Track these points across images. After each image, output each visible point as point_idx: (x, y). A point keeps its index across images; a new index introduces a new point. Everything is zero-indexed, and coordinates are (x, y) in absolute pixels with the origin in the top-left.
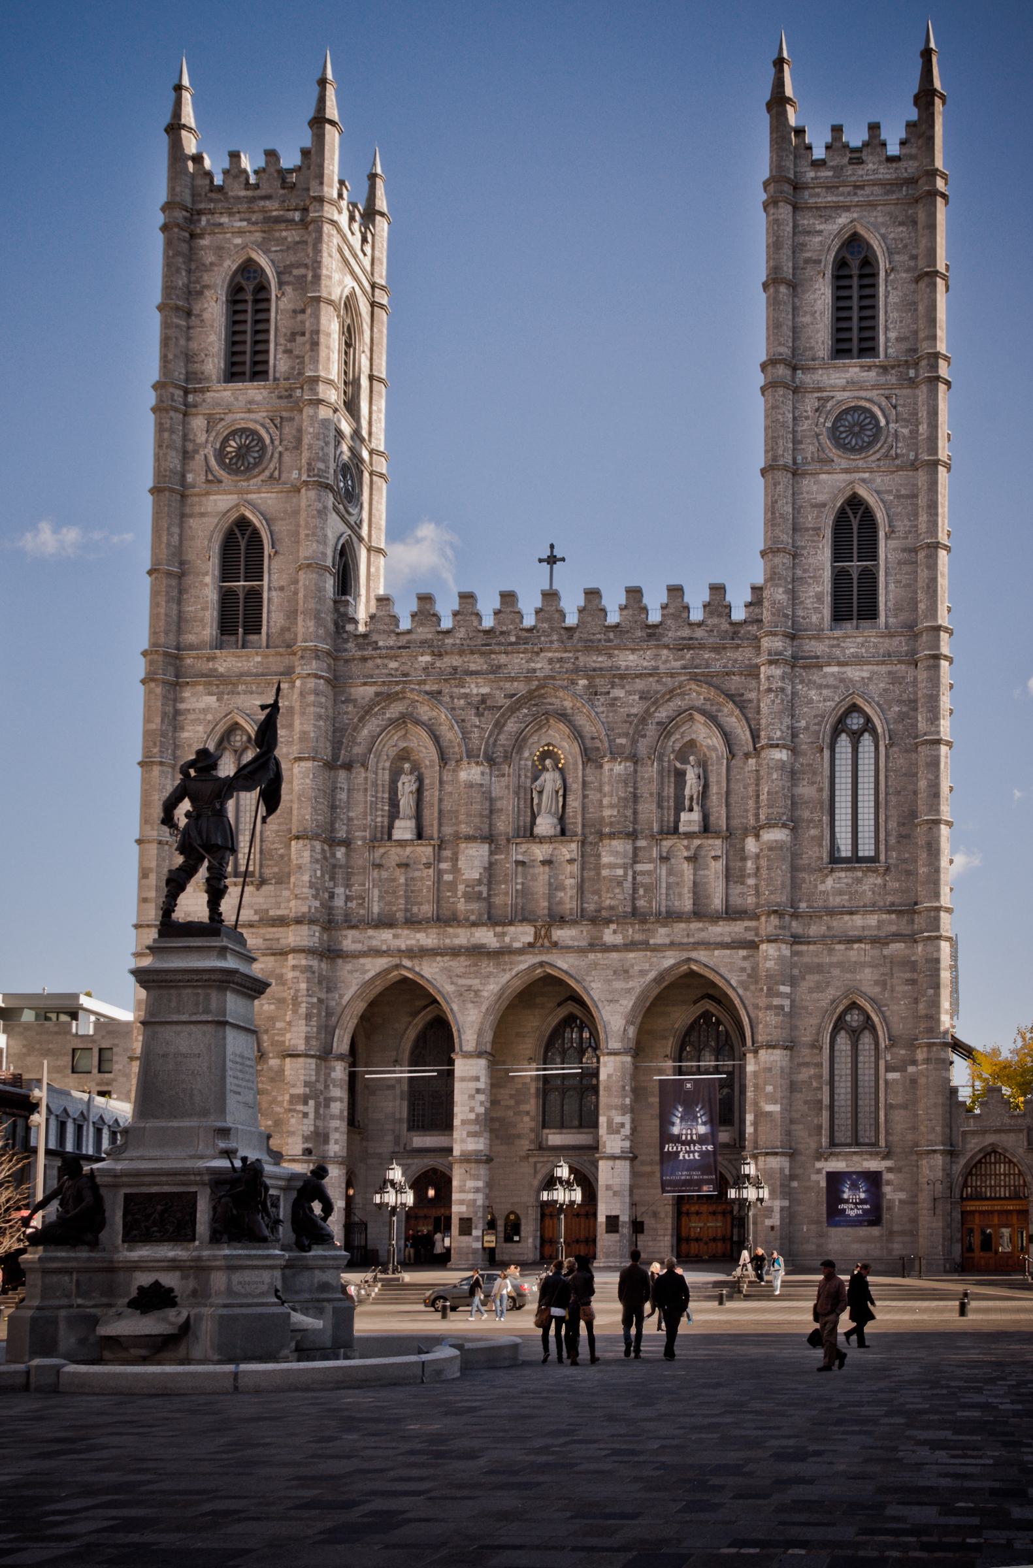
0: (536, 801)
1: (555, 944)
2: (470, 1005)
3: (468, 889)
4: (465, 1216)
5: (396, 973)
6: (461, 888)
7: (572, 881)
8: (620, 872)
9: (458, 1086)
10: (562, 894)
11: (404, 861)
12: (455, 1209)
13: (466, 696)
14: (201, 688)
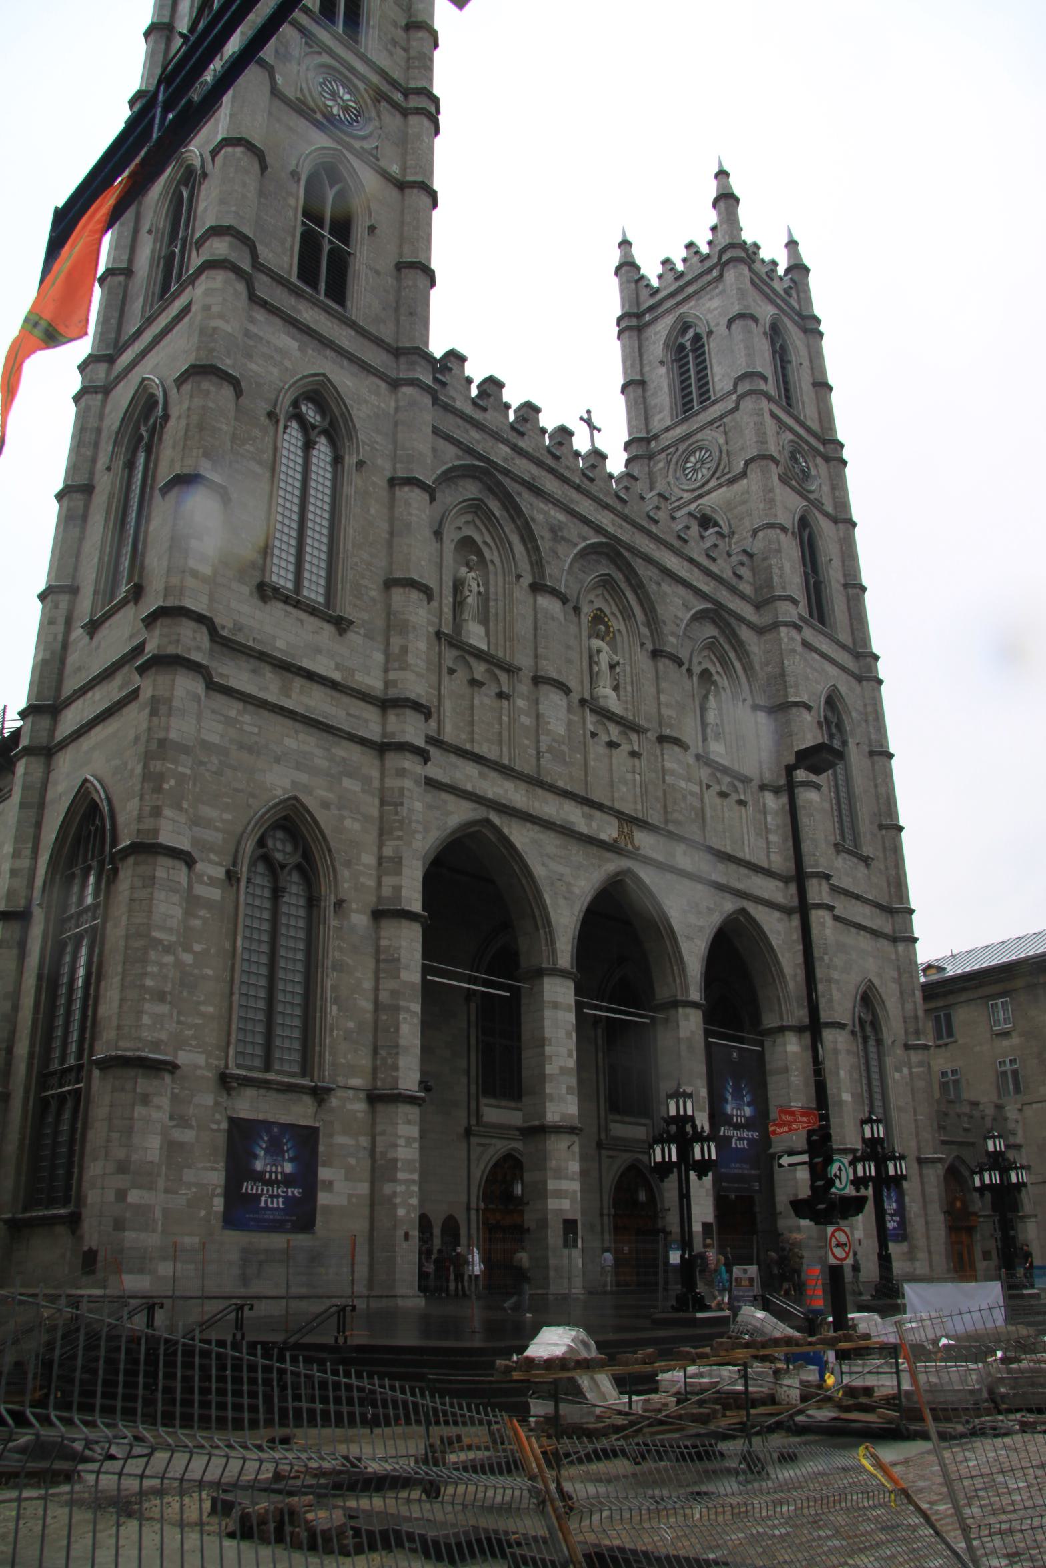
0: (596, 669)
1: (638, 849)
2: (562, 902)
3: (554, 744)
4: (570, 1216)
5: (476, 828)
6: (545, 740)
7: (637, 776)
8: (683, 784)
9: (548, 1013)
10: (624, 789)
11: (478, 677)
12: (553, 1204)
13: (546, 513)
14: (277, 321)
